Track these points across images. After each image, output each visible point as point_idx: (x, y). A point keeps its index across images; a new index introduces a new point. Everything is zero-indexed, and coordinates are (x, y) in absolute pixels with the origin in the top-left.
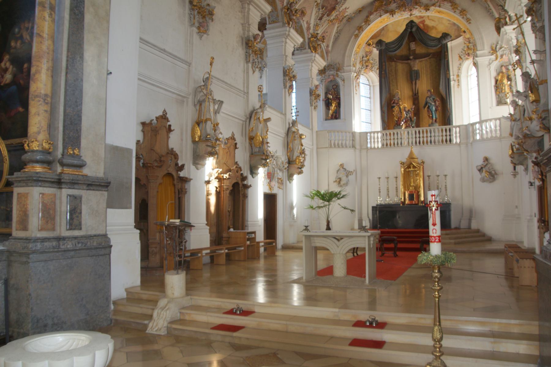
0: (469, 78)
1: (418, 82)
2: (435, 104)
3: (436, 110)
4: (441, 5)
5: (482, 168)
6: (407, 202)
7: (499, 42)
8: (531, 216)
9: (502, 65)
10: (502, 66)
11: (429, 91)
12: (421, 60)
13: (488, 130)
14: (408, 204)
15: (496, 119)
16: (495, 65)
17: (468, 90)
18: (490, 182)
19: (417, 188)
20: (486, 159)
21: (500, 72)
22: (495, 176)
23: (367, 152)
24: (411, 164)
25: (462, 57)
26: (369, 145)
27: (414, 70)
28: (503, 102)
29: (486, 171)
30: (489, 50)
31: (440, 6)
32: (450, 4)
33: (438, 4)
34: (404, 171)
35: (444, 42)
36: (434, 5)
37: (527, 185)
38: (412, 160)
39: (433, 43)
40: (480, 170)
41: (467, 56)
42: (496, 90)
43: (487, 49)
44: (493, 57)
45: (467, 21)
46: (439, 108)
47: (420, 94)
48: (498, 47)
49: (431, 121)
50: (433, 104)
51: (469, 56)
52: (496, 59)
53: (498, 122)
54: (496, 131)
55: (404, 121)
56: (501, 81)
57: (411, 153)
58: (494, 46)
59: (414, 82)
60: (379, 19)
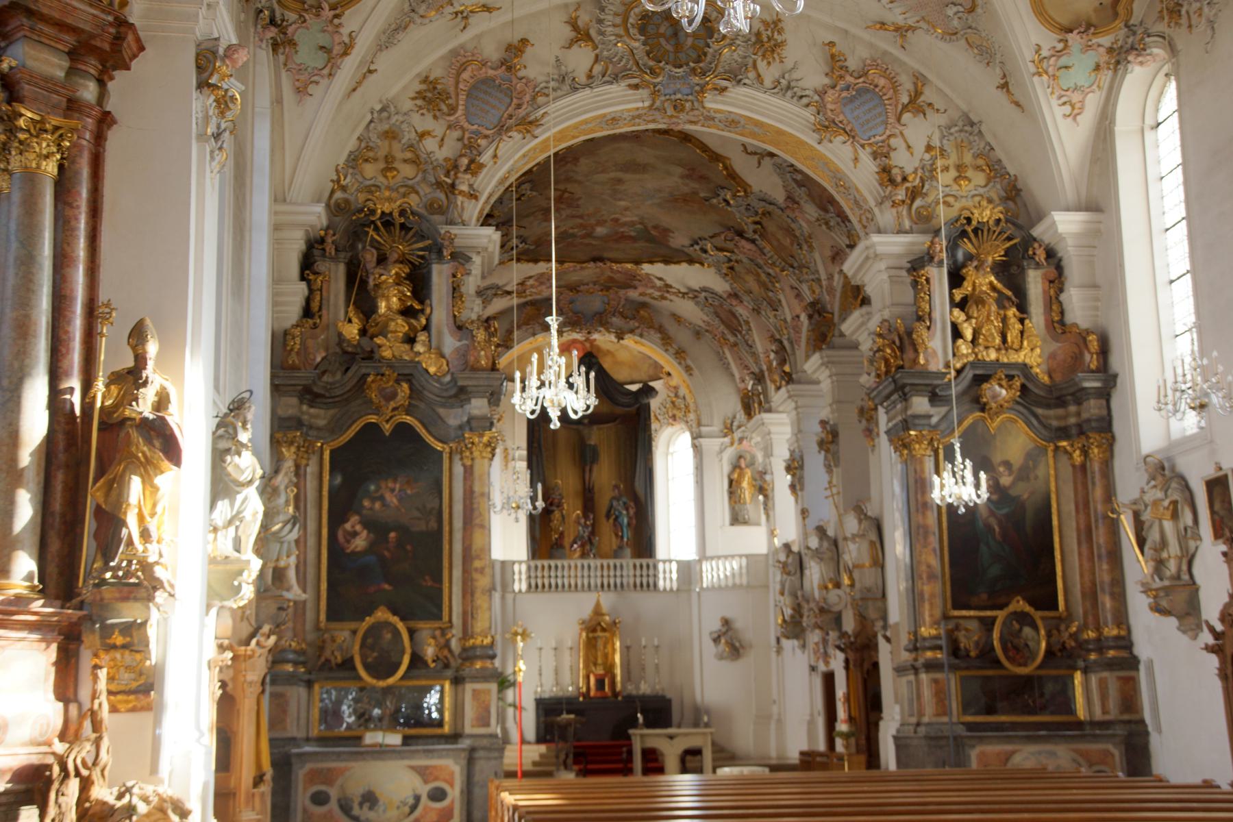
0: (670, 457)
1: (595, 468)
2: (628, 513)
3: (629, 524)
4: (645, 333)
5: (719, 637)
6: (592, 693)
7: (738, 416)
8: (812, 715)
9: (743, 454)
10: (740, 457)
11: (616, 487)
12: (602, 426)
13: (728, 574)
14: (595, 698)
15: (741, 556)
16: (729, 454)
17: (668, 480)
18: (732, 660)
19: (610, 669)
20: (726, 622)
21: (736, 466)
22: (741, 651)
23: (514, 600)
24: (599, 624)
25: (659, 417)
26: (516, 588)
27: (590, 445)
28: (740, 518)
29: (727, 642)
30: (722, 427)
31: (641, 336)
32: (659, 335)
33: (638, 331)
34: (587, 636)
35: (646, 401)
36: (632, 331)
37: (806, 669)
38: (600, 618)
39: (625, 400)
40: (716, 640)
41: (671, 421)
42: (730, 498)
43: (716, 427)
44: (727, 440)
45: (687, 371)
46: (634, 522)
47: (596, 489)
48: (735, 424)
49: (615, 542)
50: (624, 512)
51: (675, 420)
52: (732, 444)
53: (744, 561)
54: (741, 574)
55: (579, 543)
56: (739, 482)
57: (598, 605)
58: (729, 421)
59: (587, 468)
60: (531, 339)
